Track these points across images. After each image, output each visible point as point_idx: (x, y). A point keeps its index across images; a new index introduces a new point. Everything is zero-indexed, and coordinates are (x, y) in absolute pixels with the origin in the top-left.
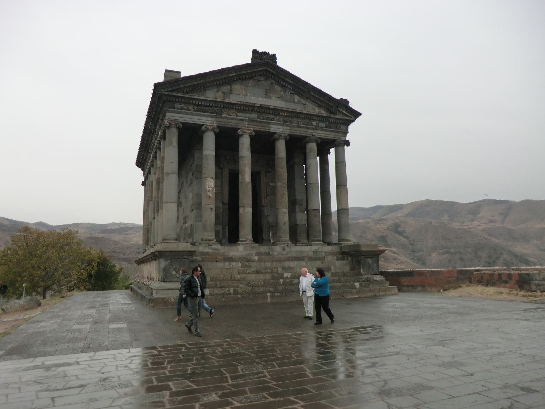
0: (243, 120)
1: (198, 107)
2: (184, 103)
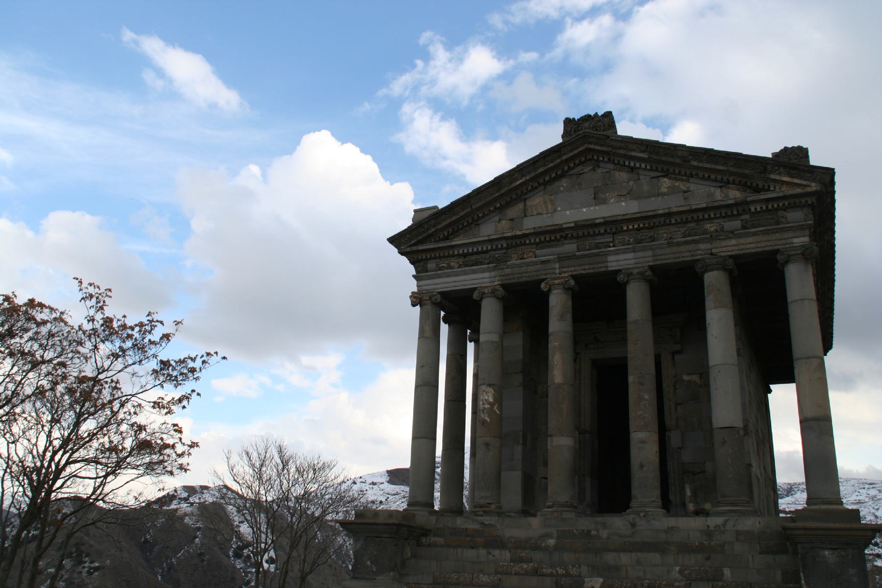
0: (548, 261)
1: (467, 259)
2: (440, 258)
